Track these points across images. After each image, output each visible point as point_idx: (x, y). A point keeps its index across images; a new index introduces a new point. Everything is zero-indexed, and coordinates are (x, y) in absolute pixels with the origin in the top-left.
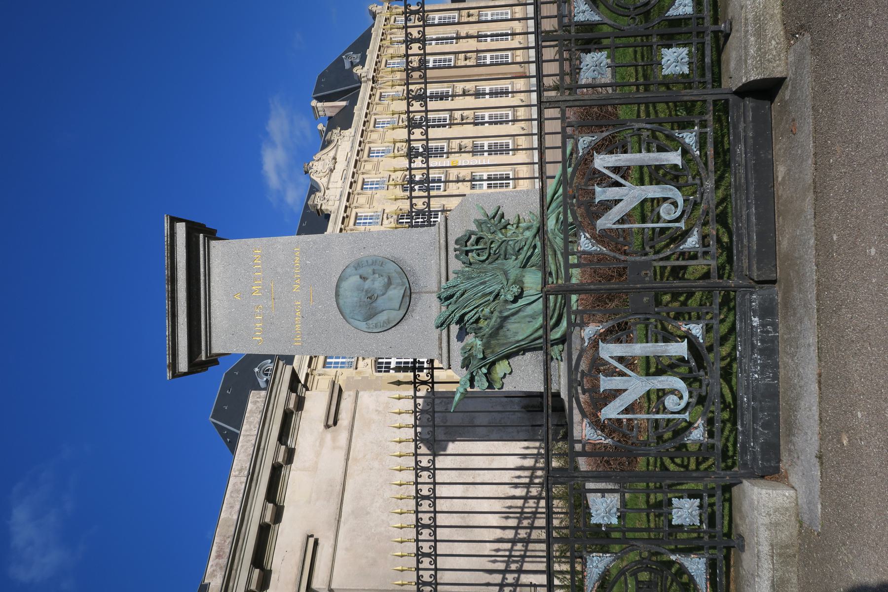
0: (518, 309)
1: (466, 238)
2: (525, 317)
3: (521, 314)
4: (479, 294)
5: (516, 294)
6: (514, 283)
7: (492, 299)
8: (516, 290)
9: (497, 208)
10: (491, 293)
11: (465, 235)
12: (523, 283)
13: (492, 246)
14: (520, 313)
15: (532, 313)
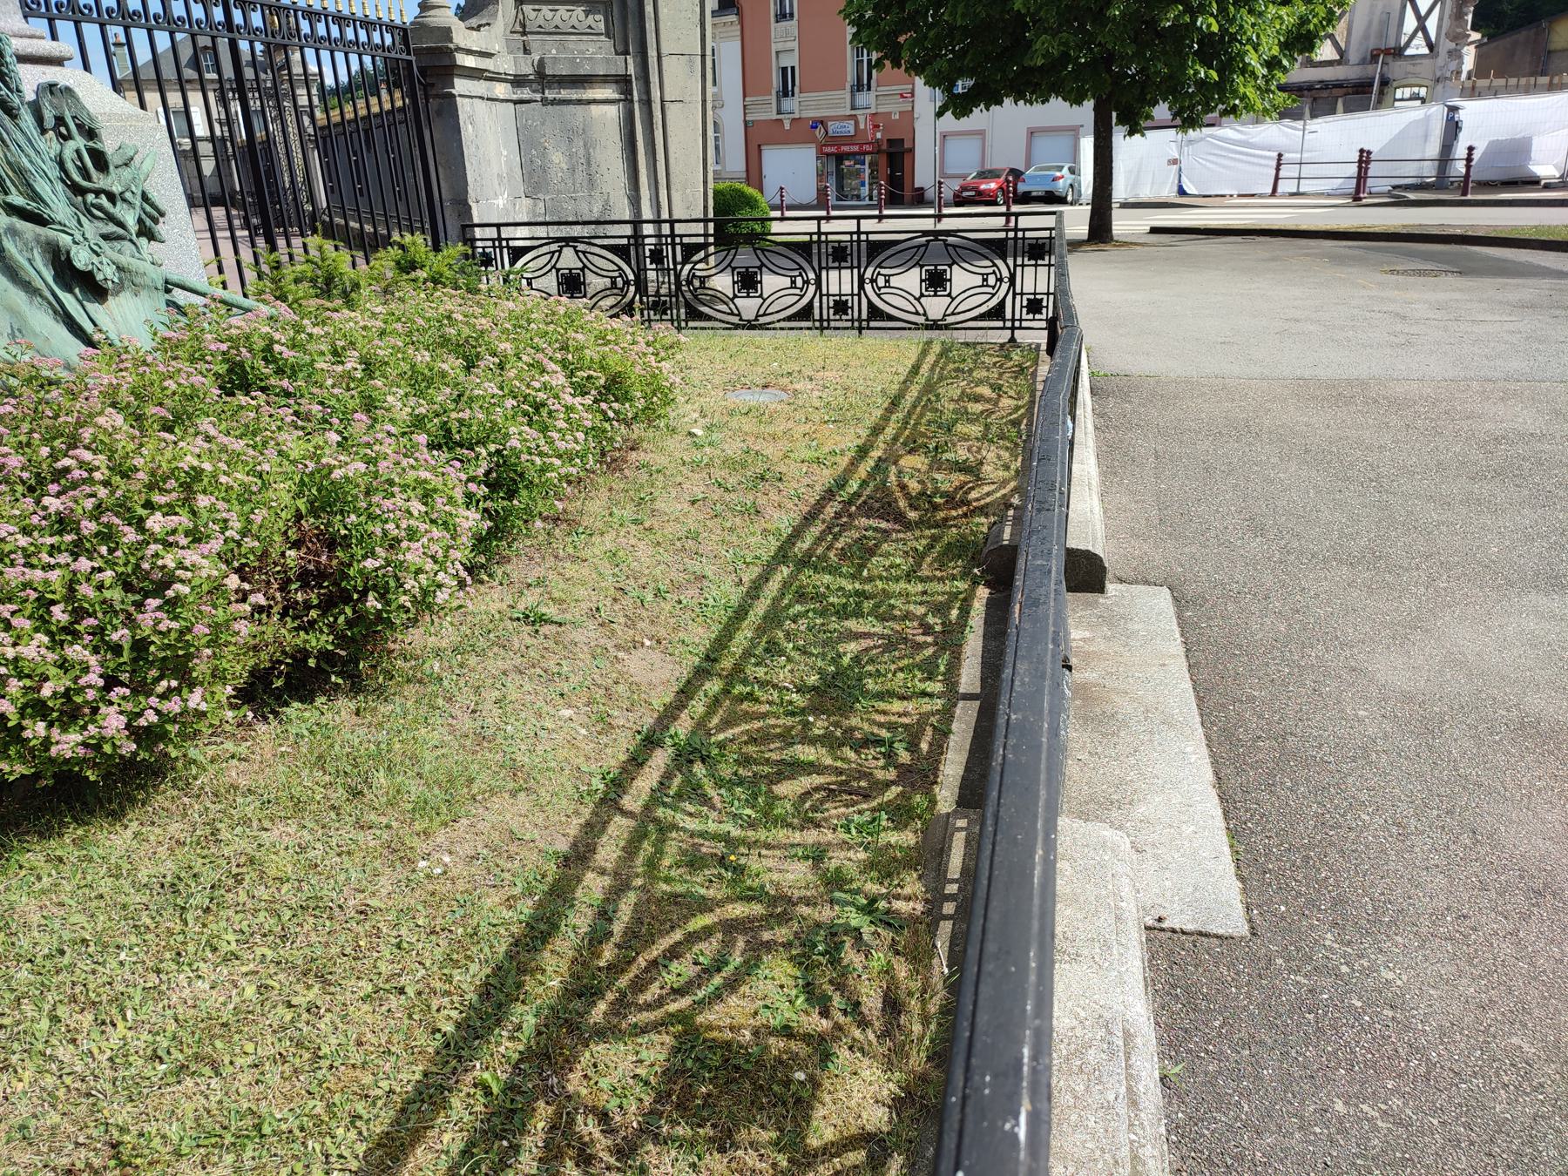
0: (39, 283)
1: (87, 122)
2: (13, 311)
3: (18, 296)
4: (25, 160)
5: (99, 277)
6: (120, 269)
7: (17, 199)
8: (107, 273)
9: (162, 205)
10: (35, 196)
11: (91, 119)
12: (117, 293)
13: (103, 196)
14: (22, 294)
15: (38, 330)
